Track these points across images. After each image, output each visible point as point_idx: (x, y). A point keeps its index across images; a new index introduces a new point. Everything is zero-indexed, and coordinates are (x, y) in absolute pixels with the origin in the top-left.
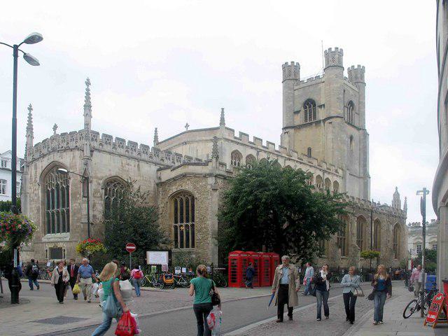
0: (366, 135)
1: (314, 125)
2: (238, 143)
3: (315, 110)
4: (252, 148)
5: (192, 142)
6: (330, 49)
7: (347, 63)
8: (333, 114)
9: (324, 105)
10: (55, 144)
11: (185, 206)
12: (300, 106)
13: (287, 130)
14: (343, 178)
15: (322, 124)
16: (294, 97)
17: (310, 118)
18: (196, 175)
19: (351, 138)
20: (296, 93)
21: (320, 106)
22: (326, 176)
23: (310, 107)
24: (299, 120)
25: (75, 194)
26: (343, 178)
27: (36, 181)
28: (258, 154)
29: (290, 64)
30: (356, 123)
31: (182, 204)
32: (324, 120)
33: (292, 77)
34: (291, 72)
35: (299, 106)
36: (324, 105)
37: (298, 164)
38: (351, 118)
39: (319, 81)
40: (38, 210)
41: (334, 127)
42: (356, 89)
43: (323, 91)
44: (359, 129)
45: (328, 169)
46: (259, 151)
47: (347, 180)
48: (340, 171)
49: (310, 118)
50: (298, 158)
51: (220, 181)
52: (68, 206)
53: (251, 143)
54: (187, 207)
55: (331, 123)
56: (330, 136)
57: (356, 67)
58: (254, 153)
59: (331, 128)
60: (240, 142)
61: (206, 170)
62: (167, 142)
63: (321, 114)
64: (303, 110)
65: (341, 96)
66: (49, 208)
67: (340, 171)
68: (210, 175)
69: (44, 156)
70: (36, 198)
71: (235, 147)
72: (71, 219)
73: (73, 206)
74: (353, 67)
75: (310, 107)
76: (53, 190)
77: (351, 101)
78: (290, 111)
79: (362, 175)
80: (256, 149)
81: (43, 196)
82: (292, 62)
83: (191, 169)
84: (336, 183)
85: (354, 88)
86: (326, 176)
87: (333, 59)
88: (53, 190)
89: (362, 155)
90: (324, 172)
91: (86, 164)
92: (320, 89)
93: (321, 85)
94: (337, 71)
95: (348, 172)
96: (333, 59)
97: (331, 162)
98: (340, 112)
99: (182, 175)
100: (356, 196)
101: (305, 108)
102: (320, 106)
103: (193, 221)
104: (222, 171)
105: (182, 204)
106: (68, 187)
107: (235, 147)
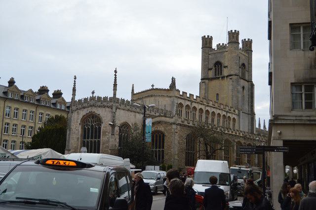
0: (252, 85)
2: (182, 99)
3: (221, 68)
4: (188, 100)
5: (156, 96)
6: (232, 31)
7: (241, 38)
8: (232, 73)
10: (92, 103)
11: (159, 137)
12: (212, 65)
13: (204, 81)
14: (239, 115)
16: (208, 59)
17: (218, 74)
18: (166, 123)
19: (243, 88)
20: (210, 56)
21: (225, 67)
22: (229, 115)
24: (211, 74)
25: (105, 132)
26: (239, 115)
27: (77, 122)
28: (191, 104)
29: (206, 37)
30: (247, 78)
31: (156, 138)
32: (227, 76)
33: (208, 45)
34: (207, 42)
35: (211, 65)
37: (212, 109)
38: (243, 74)
39: (224, 50)
40: (78, 139)
41: (233, 82)
42: (247, 55)
43: (226, 57)
44: (248, 81)
45: (229, 110)
46: (192, 102)
47: (241, 117)
48: (237, 111)
49: (218, 74)
50: (213, 105)
51: (178, 127)
52: (99, 137)
53: (188, 97)
54: (160, 139)
56: (231, 87)
57: (247, 40)
58: (189, 103)
59: (231, 83)
60: (183, 97)
61: (172, 120)
63: (226, 72)
64: (214, 67)
65: (237, 61)
66: (85, 138)
67: (237, 111)
68: (174, 124)
69: (84, 108)
70: (76, 132)
71: (180, 101)
72: (101, 146)
73: (103, 139)
74: (245, 39)
77: (244, 64)
78: (205, 67)
79: (250, 113)
80: (190, 101)
81: (82, 131)
82: (208, 36)
83: (163, 119)
84: (234, 119)
85: (245, 54)
86: (229, 115)
87: (233, 36)
88: (88, 128)
89: (250, 99)
90: (227, 112)
91: (114, 117)
92: (225, 56)
93: (226, 53)
94: (235, 45)
95: (241, 112)
96: (233, 36)
97: (230, 105)
98: (237, 72)
99: (158, 122)
100: (246, 130)
101: (215, 66)
103: (163, 148)
104: (179, 121)
105: (156, 138)
106: (100, 128)
107: (180, 101)
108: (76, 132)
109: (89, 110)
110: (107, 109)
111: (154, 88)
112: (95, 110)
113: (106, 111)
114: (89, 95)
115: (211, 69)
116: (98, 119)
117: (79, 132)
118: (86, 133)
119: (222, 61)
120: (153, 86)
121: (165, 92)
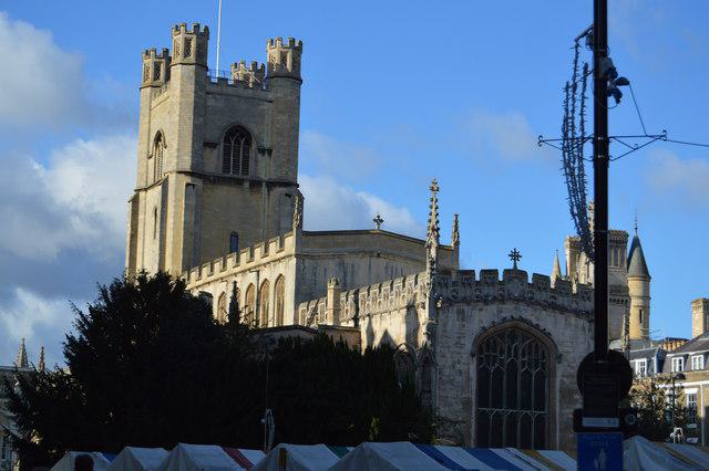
1: (247, 185)
3: (246, 151)
9: (270, 152)
15: (264, 189)
16: (205, 107)
17: (236, 166)
20: (211, 102)
21: (262, 151)
23: (237, 142)
24: (213, 162)
27: (459, 344)
32: (271, 185)
35: (215, 134)
36: (270, 152)
40: (467, 403)
49: (236, 166)
55: (289, 196)
62: (320, 239)
70: (459, 379)
75: (237, 142)
76: (498, 371)
93: (266, 106)
101: (227, 140)
102: (262, 151)
108: (459, 379)
109: (509, 310)
110: (573, 319)
111: (385, 227)
112: (529, 314)
113: (568, 324)
114: (502, 264)
115: (211, 145)
116: (540, 348)
117: (469, 379)
118: (489, 387)
119: (254, 128)
120: (379, 221)
121: (386, 238)
